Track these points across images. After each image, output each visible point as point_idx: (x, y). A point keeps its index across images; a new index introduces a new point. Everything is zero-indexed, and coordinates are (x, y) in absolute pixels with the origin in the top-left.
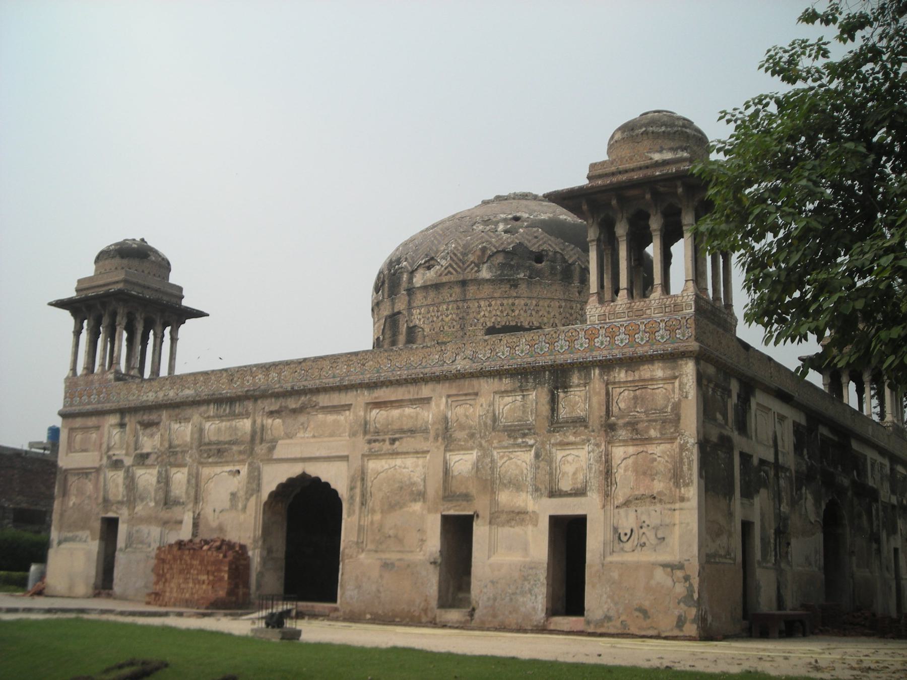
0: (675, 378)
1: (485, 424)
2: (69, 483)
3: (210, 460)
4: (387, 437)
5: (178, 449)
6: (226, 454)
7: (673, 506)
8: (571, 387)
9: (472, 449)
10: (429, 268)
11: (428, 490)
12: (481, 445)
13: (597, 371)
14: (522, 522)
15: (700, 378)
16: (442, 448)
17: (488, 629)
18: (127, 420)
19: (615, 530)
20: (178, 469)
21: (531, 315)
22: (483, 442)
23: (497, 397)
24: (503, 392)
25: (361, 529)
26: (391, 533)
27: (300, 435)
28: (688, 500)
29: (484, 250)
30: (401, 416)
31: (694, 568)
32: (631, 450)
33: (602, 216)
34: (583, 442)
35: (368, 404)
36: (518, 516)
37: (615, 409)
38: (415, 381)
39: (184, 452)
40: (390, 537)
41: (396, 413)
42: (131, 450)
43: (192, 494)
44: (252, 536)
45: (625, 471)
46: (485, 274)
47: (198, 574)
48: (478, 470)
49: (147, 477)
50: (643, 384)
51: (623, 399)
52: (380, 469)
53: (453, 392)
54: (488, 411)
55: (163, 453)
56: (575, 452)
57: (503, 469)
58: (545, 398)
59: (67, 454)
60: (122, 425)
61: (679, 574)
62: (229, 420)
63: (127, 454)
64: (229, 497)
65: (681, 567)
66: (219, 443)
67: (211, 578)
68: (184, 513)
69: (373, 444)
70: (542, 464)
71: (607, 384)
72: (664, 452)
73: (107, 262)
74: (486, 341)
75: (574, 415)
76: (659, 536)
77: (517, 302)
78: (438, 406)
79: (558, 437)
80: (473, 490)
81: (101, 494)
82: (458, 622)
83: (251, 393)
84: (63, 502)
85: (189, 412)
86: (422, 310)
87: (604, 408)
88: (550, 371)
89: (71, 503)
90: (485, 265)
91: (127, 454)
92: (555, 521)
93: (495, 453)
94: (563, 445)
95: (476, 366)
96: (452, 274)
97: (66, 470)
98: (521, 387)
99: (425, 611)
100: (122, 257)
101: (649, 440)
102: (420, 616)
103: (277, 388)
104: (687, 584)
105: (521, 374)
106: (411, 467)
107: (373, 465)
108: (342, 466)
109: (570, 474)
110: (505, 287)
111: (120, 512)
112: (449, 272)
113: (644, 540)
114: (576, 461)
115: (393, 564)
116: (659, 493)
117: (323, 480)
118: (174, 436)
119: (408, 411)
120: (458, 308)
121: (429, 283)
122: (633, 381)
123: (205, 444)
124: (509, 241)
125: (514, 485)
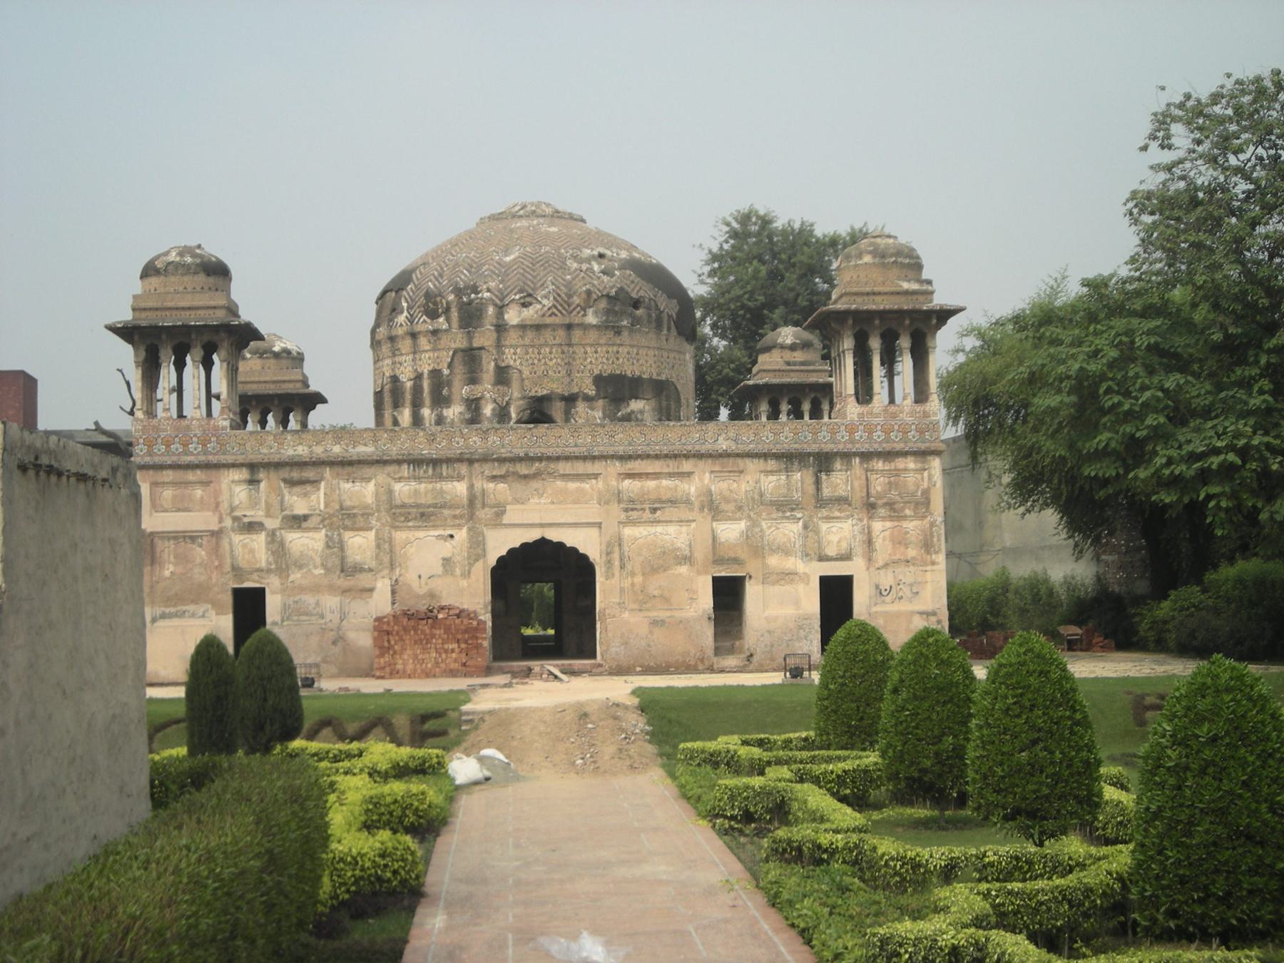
1: (753, 499)
2: (158, 550)
3: (411, 524)
4: (647, 506)
9: (740, 519)
10: (525, 305)
11: (696, 555)
13: (857, 460)
16: (710, 518)
17: (767, 671)
18: (261, 475)
19: (877, 587)
25: (622, 590)
26: (656, 593)
27: (534, 500)
29: (589, 293)
30: (658, 487)
32: (888, 524)
34: (848, 517)
36: (788, 576)
37: (873, 492)
38: (676, 456)
39: (366, 515)
41: (651, 484)
43: (386, 559)
44: (482, 601)
45: (884, 539)
46: (591, 319)
49: (306, 541)
50: (897, 472)
51: (878, 484)
52: (638, 535)
55: (331, 516)
56: (839, 525)
57: (771, 538)
58: (810, 480)
60: (253, 482)
61: (933, 619)
63: (268, 515)
65: (934, 614)
66: (418, 506)
67: (463, 646)
70: (810, 534)
71: (867, 471)
73: (186, 279)
78: (701, 480)
79: (824, 512)
80: (742, 554)
81: (228, 561)
85: (368, 471)
89: (167, 573)
91: (268, 515)
92: (826, 582)
93: (763, 523)
95: (742, 448)
97: (152, 533)
99: (702, 660)
101: (905, 518)
102: (696, 666)
103: (504, 452)
106: (673, 534)
107: (628, 532)
108: (594, 532)
110: (610, 334)
112: (553, 314)
114: (839, 532)
115: (663, 622)
116: (913, 558)
118: (345, 497)
119: (665, 482)
120: (563, 352)
123: (397, 507)
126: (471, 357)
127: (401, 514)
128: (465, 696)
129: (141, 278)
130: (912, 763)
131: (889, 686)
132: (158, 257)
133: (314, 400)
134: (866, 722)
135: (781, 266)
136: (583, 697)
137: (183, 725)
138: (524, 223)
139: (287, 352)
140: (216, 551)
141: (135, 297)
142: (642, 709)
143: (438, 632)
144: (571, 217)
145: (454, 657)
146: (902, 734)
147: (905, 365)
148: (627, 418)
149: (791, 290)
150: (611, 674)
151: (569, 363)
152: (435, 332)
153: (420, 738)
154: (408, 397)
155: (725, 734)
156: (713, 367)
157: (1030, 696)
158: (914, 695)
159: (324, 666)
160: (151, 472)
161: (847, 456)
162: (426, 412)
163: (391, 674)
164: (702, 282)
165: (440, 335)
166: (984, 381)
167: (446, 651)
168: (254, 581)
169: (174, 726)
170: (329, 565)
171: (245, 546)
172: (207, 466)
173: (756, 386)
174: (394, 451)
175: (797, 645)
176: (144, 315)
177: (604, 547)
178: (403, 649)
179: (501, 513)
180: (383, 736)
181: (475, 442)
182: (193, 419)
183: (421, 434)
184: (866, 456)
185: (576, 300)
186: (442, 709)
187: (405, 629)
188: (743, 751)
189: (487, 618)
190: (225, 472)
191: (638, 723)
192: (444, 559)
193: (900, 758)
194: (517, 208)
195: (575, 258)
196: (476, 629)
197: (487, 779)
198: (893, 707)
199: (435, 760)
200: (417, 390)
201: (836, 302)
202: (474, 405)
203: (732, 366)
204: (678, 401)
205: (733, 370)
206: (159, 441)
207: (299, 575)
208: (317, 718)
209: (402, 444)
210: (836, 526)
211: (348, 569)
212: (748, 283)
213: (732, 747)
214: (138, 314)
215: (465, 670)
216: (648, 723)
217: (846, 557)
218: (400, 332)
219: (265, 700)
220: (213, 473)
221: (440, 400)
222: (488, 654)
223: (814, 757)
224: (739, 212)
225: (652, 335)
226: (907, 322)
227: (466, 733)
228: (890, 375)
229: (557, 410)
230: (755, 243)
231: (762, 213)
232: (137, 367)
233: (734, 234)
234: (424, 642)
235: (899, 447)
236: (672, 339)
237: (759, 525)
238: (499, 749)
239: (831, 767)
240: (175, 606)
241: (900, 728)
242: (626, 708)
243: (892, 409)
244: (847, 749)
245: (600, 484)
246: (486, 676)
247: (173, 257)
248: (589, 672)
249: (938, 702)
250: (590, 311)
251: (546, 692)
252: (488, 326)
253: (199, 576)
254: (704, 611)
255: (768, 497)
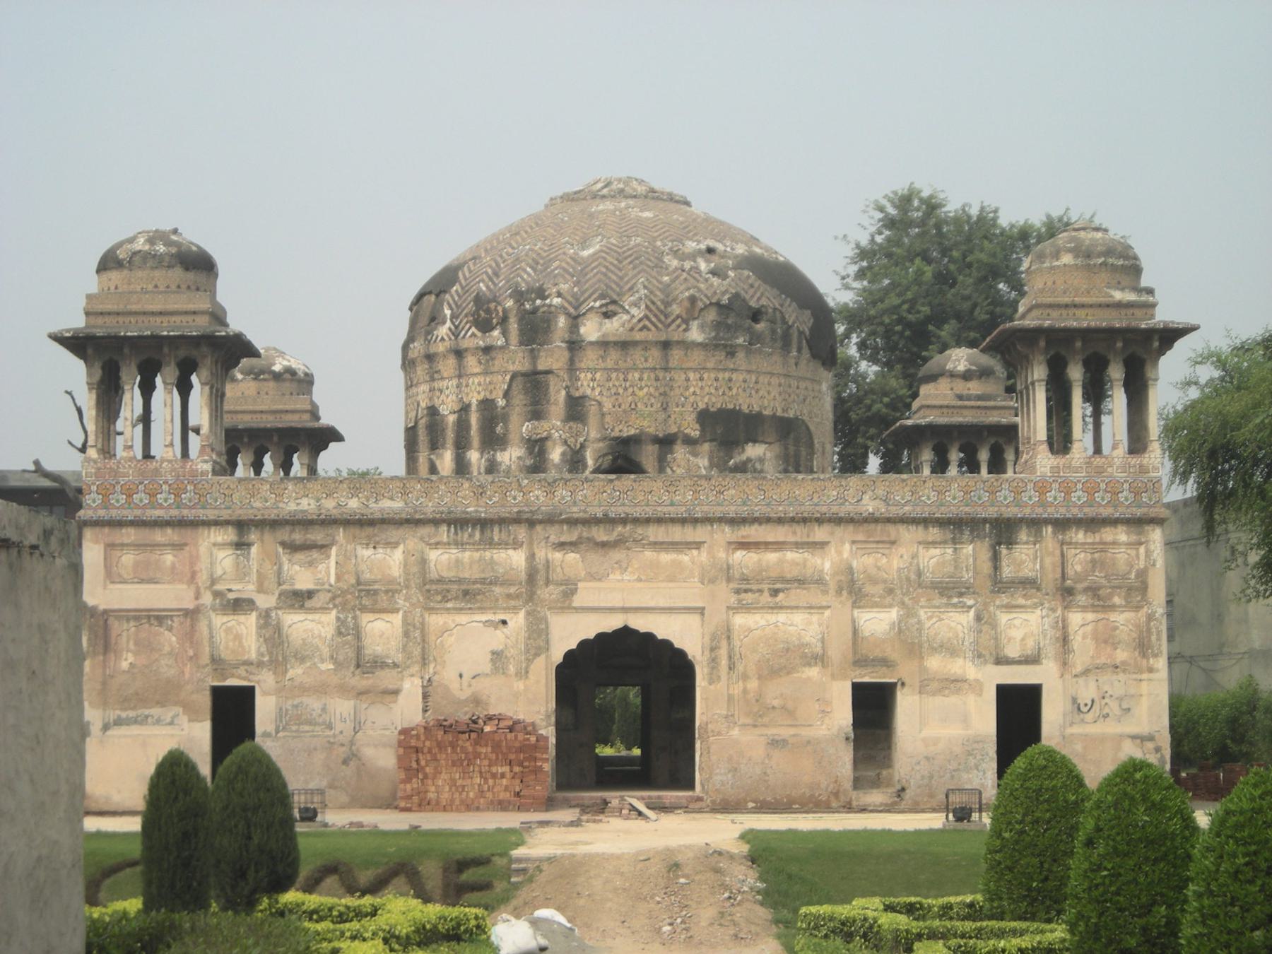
0: (1141, 544)
1: (908, 579)
2: (114, 633)
3: (450, 605)
4: (765, 587)
5: (376, 587)
6: (479, 597)
7: (1139, 677)
8: (1017, 543)
9: (891, 606)
10: (607, 315)
12: (903, 603)
13: (1050, 529)
14: (958, 691)
15: (1168, 544)
16: (849, 604)
17: (923, 811)
18: (253, 536)
19: (1074, 700)
20: (377, 616)
21: (750, 396)
22: (906, 599)
23: (921, 547)
24: (929, 543)
25: (730, 698)
26: (776, 703)
27: (616, 576)
28: (1158, 671)
29: (693, 300)
30: (781, 561)
31: (1165, 740)
32: (1090, 616)
33: (1052, 353)
34: (1035, 606)
35: (730, 543)
36: (954, 684)
38: (805, 521)
39: (391, 593)
40: (774, 708)
41: (772, 557)
42: (271, 582)
43: (417, 652)
44: (543, 710)
45: (1084, 638)
46: (696, 334)
47: (490, 766)
48: (900, 631)
50: (1104, 546)
51: (1078, 562)
52: (753, 626)
53: (861, 537)
54: (911, 564)
55: (344, 593)
56: (1024, 616)
58: (985, 554)
59: (105, 587)
60: (241, 545)
61: (1150, 745)
62: (478, 550)
63: (261, 589)
64: (489, 656)
65: (1151, 738)
66: (460, 581)
67: (517, 769)
68: (402, 679)
69: (743, 595)
70: (985, 628)
71: (1062, 544)
72: (1128, 621)
73: (157, 273)
74: (904, 481)
75: (1021, 574)
76: (1125, 706)
77: (734, 376)
78: (839, 553)
79: (1004, 599)
81: (207, 649)
82: (882, 804)
83: (526, 516)
84: (104, 661)
85: (393, 533)
86: (598, 375)
87: (1059, 570)
88: (991, 524)
89: (125, 665)
90: (696, 323)
91: (261, 589)
93: (922, 612)
94: (1009, 607)
95: (894, 511)
96: (649, 330)
97: (105, 612)
98: (954, 539)
99: (836, 795)
100: (187, 269)
101: (1113, 608)
103: (576, 512)
104: (1158, 755)
105: (954, 524)
106: (799, 624)
107: (739, 620)
108: (694, 619)
109: (1018, 640)
110: (721, 355)
111: (256, 678)
112: (645, 327)
113: (1106, 711)
114: (1024, 625)
115: (784, 740)
116: (1123, 663)
117: (660, 637)
118: (363, 567)
119: (790, 555)
120: (657, 379)
121: (611, 339)
122: (1093, 544)
123: (432, 582)
124: (721, 288)
125: (948, 649)
126: (534, 384)
127: (437, 593)
128: (517, 836)
129: (98, 271)
130: (1110, 942)
131: (1081, 836)
132: (120, 245)
133: (324, 437)
134: (1052, 884)
135: (952, 267)
136: (674, 842)
137: (139, 869)
138: (608, 205)
139: (291, 372)
140: (190, 636)
141: (89, 297)
142: (753, 859)
143: (484, 750)
144: (671, 198)
145: (504, 786)
146: (1098, 902)
147: (1118, 401)
148: (742, 468)
149: (968, 298)
150: (714, 810)
151: (664, 394)
152: (487, 350)
153: (455, 893)
154: (450, 435)
155: (863, 896)
156: (858, 400)
157: (1267, 854)
158: (1115, 848)
159: (330, 793)
160: (106, 530)
161: (1035, 524)
162: (474, 456)
163: (420, 805)
164: (847, 287)
165: (493, 354)
166: (1224, 425)
167: (494, 776)
168: (239, 677)
169: (128, 870)
170: (341, 658)
171: (228, 631)
172: (181, 523)
173: (917, 428)
174: (429, 507)
175: (965, 776)
176: (100, 321)
177: (707, 639)
178: (437, 773)
179: (570, 592)
180: (406, 888)
181: (537, 497)
182: (163, 460)
183: (466, 485)
184: (1062, 524)
185: (676, 309)
186: (486, 853)
187: (440, 746)
188: (886, 920)
189: (549, 732)
190: (203, 532)
191: (747, 878)
192: (493, 653)
193: (1095, 933)
194: (599, 185)
195: (675, 253)
196: (535, 747)
197: (543, 949)
198: (1086, 865)
199: (473, 923)
200: (462, 426)
201: (1023, 317)
202: (537, 447)
203: (886, 400)
204: (811, 445)
205: (887, 406)
206: (118, 488)
207: (299, 671)
208: (319, 863)
209: (441, 498)
210: (1019, 618)
211: (365, 664)
212: (908, 289)
213: (870, 914)
214: (93, 320)
215: (519, 802)
216: (761, 879)
217: (1032, 660)
218: (441, 348)
219: (250, 838)
220: (188, 533)
221: (493, 441)
222: (550, 781)
223: (980, 930)
224: (895, 193)
225: (777, 358)
226: (1119, 345)
227: (516, 886)
228: (1097, 414)
229: (648, 456)
230: (918, 234)
231: (925, 194)
232: (90, 390)
233: (890, 223)
234: (465, 763)
235: (1106, 512)
236: (803, 363)
237: (916, 615)
238: (558, 909)
239: (1002, 944)
240: (134, 708)
241: (1095, 893)
242: (732, 857)
243: (1098, 461)
244: (1026, 919)
245: (702, 556)
246: (547, 810)
247: (140, 244)
248: (686, 809)
249: (1147, 859)
250: (694, 325)
251: (627, 835)
252: (558, 341)
253: (167, 669)
254: (840, 729)
255: (928, 577)
